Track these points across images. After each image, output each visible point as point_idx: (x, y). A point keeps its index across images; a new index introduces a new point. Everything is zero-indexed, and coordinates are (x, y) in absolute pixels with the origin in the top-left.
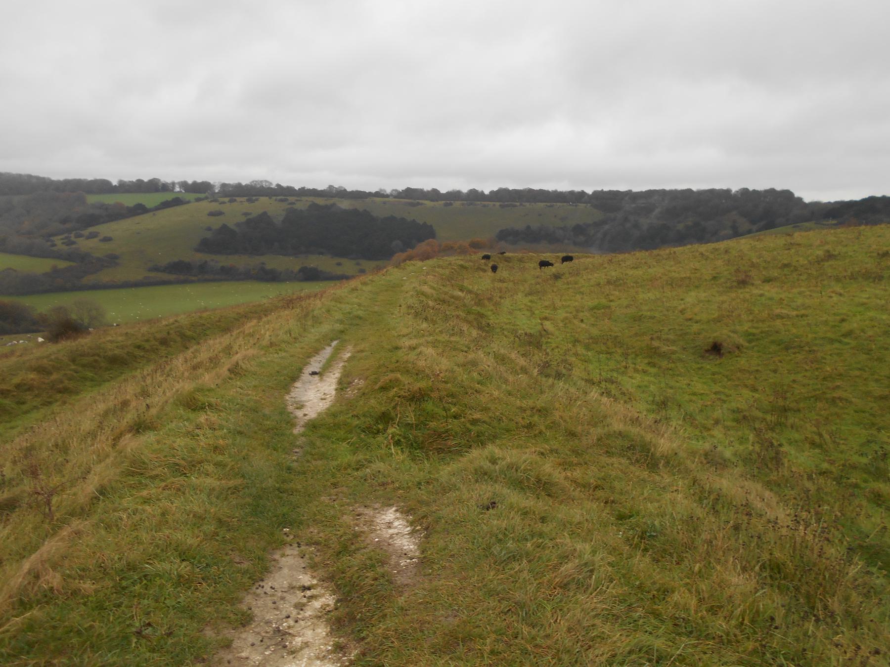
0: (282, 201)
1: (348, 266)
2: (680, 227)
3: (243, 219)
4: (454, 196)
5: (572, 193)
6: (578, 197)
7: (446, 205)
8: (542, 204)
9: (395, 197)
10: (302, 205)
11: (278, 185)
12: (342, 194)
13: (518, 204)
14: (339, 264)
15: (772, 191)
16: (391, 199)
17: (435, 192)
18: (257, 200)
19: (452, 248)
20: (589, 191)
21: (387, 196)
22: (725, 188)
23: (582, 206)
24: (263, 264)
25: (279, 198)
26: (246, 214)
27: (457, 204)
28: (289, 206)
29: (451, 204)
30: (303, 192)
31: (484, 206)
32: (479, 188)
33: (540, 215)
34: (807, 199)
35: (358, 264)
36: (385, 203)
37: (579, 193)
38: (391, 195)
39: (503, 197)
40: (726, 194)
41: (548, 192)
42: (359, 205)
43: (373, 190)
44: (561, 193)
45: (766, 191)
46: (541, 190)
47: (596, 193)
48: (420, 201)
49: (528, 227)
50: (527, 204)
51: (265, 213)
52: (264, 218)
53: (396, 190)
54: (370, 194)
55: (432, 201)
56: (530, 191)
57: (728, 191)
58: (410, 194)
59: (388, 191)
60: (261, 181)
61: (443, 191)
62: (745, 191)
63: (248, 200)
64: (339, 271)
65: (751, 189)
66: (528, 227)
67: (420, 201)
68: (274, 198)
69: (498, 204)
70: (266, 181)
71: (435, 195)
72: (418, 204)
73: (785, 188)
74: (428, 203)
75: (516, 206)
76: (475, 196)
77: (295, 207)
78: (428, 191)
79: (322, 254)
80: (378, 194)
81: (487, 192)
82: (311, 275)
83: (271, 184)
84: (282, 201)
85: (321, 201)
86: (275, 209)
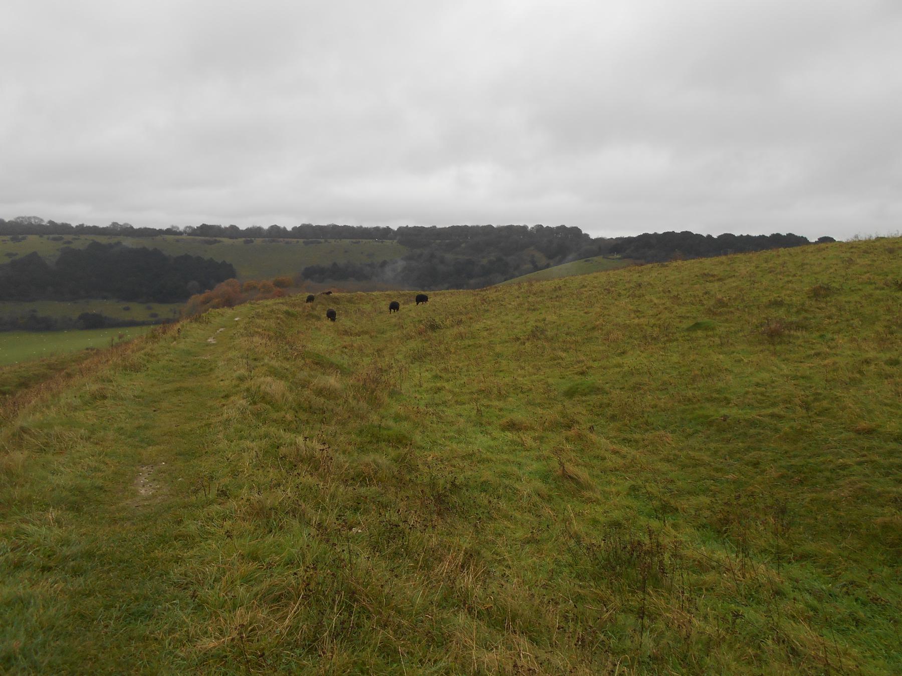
0: (55, 239)
1: (138, 311)
2: (485, 261)
3: (7, 260)
4: (254, 233)
7: (246, 242)
8: (347, 241)
9: (189, 234)
10: (81, 244)
11: (51, 222)
12: (128, 231)
13: (323, 240)
14: (127, 309)
15: (563, 228)
16: (184, 236)
17: (233, 228)
18: (24, 239)
19: (255, 288)
20: (395, 227)
21: (181, 233)
22: (522, 225)
23: (388, 242)
24: (34, 311)
25: (51, 236)
26: (9, 255)
27: (258, 241)
28: (66, 245)
29: (252, 242)
30: (82, 230)
31: (287, 243)
32: (281, 224)
34: (593, 235)
35: (149, 308)
36: (177, 241)
37: (384, 229)
38: (185, 232)
39: (307, 233)
40: (522, 230)
41: (353, 228)
42: (147, 243)
43: (164, 228)
44: (366, 229)
45: (558, 228)
47: (400, 229)
48: (218, 239)
49: (335, 264)
50: (333, 241)
51: (35, 254)
52: (33, 258)
53: (190, 227)
54: (161, 232)
55: (231, 238)
56: (335, 227)
57: (525, 227)
58: (205, 230)
59: (182, 228)
60: (29, 218)
61: (243, 226)
62: (540, 228)
63: (12, 239)
64: (127, 316)
66: (335, 264)
67: (218, 239)
68: (46, 236)
69: (301, 241)
70: (35, 218)
71: (233, 232)
72: (216, 241)
74: (226, 241)
76: (276, 232)
77: (73, 246)
78: (226, 228)
79: (105, 298)
80: (169, 232)
81: (289, 229)
82: (94, 323)
83: (42, 220)
84: (55, 239)
85: (103, 240)
86: (48, 249)
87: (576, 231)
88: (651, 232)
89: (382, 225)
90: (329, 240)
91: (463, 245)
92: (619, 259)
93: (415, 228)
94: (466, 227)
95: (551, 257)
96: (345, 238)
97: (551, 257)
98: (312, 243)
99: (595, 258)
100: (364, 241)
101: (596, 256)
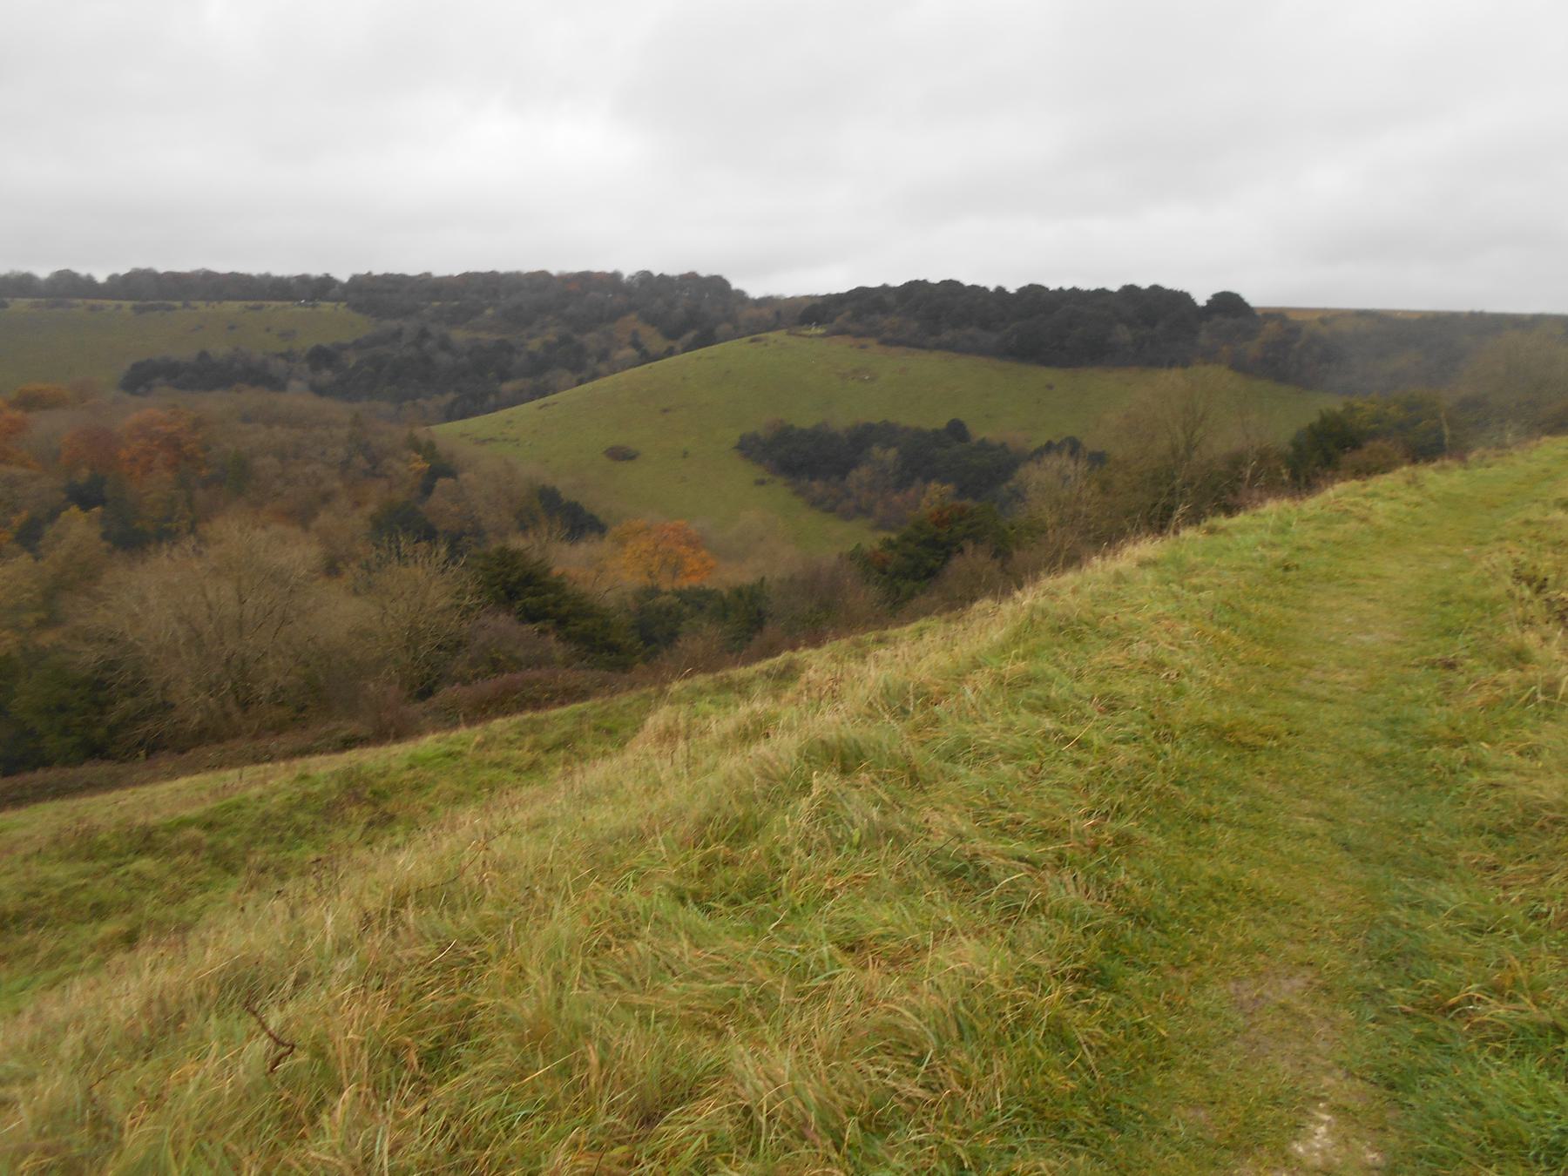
2: (535, 345)
5: (304, 280)
6: (318, 289)
8: (235, 306)
13: (178, 304)
15: (691, 278)
20: (343, 276)
22: (609, 270)
23: (326, 307)
27: (21, 304)
31: (93, 308)
33: (232, 328)
34: (755, 291)
40: (610, 281)
46: (232, 274)
47: (355, 279)
50: (201, 304)
57: (616, 276)
62: (645, 277)
65: (656, 273)
69: (127, 304)
73: (715, 273)
75: (175, 308)
76: (69, 287)
87: (717, 285)
88: (874, 282)
89: (316, 271)
90: (193, 303)
91: (489, 312)
92: (823, 336)
93: (387, 278)
94: (493, 274)
95: (673, 334)
96: (229, 298)
97: (673, 334)
98: (153, 308)
99: (772, 335)
100: (274, 304)
101: (769, 330)
